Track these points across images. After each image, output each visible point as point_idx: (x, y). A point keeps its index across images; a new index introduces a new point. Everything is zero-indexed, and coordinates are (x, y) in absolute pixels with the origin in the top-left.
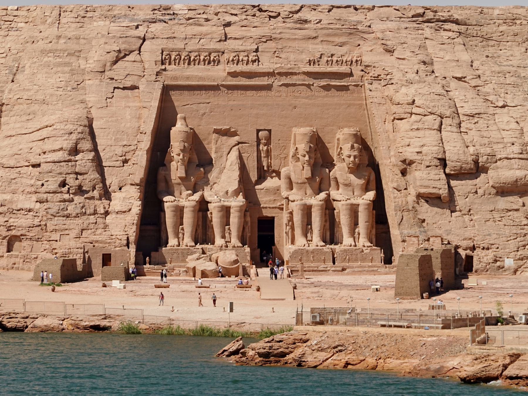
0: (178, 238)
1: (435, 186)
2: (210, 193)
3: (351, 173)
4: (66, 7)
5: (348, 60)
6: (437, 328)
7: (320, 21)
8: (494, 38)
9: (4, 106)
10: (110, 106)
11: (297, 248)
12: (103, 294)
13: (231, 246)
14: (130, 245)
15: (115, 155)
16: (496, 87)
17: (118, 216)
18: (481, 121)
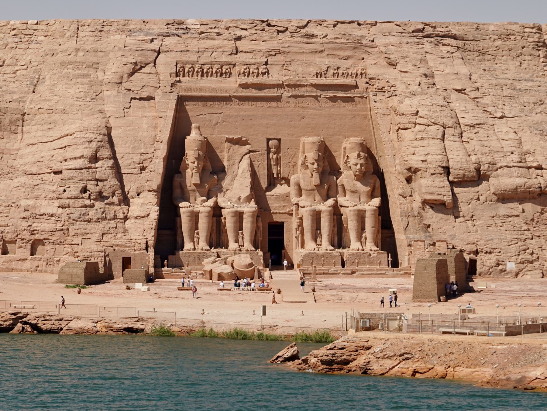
0: (194, 242)
1: (440, 193)
2: (224, 199)
3: (357, 180)
4: (83, 22)
5: (354, 72)
6: (500, 335)
7: (326, 36)
8: (489, 53)
9: (26, 116)
11: (308, 252)
12: (127, 296)
13: (245, 250)
14: (149, 249)
15: (132, 163)
16: (494, 99)
17: (137, 221)
18: (481, 131)
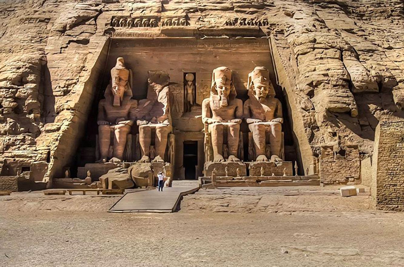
10: (63, 53)
15: (58, 87)
